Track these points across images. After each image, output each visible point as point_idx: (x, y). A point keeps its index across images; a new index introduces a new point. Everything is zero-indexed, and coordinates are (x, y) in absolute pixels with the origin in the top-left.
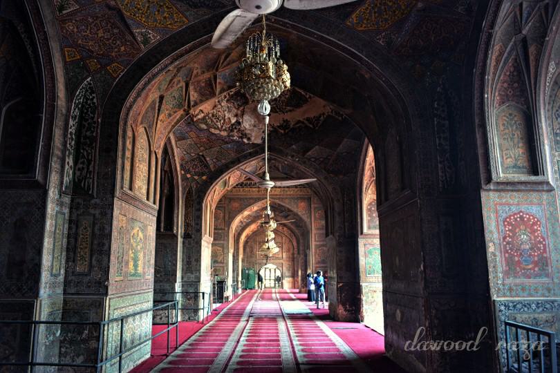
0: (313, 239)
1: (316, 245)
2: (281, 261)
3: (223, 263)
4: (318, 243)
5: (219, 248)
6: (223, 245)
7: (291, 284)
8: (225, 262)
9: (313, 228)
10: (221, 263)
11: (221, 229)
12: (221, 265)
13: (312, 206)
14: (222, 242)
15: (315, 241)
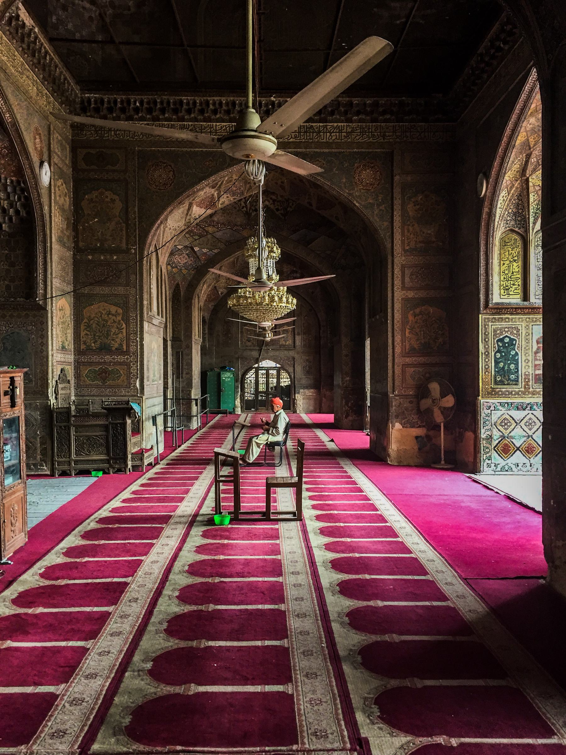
0: (397, 282)
1: (406, 300)
2: (292, 353)
3: (127, 353)
4: (411, 294)
5: (113, 309)
6: (126, 296)
7: (312, 402)
8: (132, 349)
9: (398, 248)
10: (120, 351)
11: (118, 251)
12: (120, 358)
13: (397, 178)
14: (121, 290)
15: (403, 288)
